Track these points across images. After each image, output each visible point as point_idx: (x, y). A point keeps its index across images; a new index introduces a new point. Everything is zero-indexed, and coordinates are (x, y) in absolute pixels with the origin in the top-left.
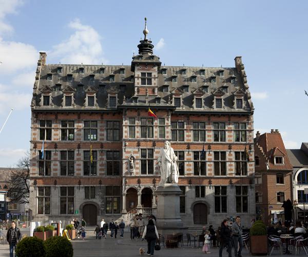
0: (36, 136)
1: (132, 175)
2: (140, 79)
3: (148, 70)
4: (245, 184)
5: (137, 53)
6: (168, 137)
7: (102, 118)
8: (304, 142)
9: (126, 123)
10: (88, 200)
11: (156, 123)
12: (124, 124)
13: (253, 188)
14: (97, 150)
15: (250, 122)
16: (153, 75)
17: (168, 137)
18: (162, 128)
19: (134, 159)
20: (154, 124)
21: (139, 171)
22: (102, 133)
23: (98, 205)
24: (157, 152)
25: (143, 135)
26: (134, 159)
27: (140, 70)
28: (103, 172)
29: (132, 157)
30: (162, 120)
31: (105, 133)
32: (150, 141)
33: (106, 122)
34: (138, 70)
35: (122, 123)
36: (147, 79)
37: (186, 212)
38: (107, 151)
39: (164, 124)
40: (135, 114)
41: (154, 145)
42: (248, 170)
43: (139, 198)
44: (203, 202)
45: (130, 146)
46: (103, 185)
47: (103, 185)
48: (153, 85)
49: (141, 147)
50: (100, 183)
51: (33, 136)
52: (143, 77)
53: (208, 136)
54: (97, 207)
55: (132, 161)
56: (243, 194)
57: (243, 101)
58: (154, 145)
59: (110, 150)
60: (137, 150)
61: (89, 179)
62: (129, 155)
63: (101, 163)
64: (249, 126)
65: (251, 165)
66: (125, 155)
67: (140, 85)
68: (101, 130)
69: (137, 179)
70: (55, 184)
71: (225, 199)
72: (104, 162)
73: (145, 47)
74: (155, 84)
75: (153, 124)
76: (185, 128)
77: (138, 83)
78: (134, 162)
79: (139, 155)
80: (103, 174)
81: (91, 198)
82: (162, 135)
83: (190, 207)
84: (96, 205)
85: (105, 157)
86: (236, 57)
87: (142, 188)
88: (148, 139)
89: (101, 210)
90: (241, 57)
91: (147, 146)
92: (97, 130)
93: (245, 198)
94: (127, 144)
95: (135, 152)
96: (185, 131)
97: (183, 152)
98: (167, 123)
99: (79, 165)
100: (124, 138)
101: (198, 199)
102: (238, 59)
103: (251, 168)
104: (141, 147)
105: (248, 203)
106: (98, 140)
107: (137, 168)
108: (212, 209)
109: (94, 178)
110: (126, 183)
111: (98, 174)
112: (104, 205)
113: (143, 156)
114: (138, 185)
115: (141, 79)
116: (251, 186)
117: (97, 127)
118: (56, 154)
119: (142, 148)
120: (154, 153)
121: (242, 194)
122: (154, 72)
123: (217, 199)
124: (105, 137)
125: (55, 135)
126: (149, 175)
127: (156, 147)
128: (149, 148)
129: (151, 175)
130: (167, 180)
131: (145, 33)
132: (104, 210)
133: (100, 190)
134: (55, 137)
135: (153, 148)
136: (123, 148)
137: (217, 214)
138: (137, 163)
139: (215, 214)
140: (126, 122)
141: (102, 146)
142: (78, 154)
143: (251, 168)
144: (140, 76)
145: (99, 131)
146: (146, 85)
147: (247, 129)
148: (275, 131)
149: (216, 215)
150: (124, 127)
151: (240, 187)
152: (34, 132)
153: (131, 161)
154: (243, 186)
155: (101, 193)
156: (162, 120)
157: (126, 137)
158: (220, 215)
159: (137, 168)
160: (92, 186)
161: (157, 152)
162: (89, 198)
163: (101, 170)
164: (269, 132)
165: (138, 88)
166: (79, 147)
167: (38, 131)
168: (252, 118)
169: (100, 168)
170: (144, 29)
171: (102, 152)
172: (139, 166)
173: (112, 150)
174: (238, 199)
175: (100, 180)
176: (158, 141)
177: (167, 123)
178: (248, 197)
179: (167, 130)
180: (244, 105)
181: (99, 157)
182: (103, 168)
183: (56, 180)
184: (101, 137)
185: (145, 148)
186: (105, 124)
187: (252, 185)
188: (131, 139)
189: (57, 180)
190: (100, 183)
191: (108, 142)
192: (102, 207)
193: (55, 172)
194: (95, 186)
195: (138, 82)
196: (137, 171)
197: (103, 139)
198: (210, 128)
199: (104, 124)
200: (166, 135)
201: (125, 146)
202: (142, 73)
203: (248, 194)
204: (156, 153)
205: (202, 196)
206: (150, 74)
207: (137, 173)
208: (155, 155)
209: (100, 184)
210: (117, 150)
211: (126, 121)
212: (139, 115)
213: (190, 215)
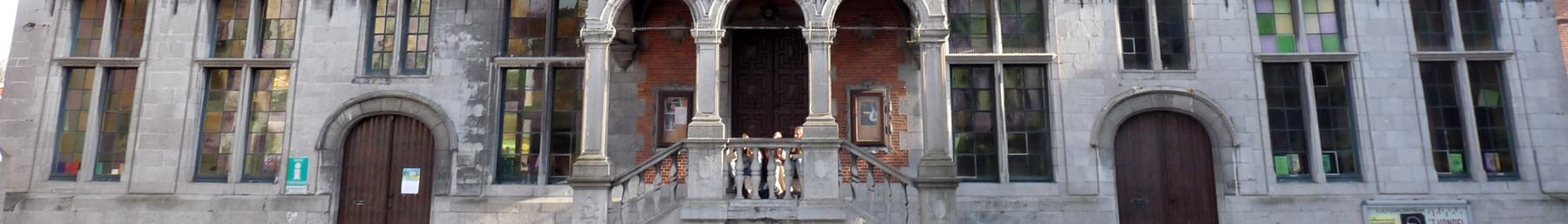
10: (379, 87)
23: (444, 119)
37: (1059, 175)
43: (709, 63)
44: (1177, 103)
54: (439, 133)
56: (1469, 42)
81: (405, 70)
83: (1086, 137)
84: (431, 121)
89: (461, 160)
93: (1489, 74)
101: (1138, 82)
105: (1517, 106)
108: (1249, 158)
112: (481, 121)
121: (1458, 45)
123: (1280, 78)
132: (480, 158)
137: (1298, 189)
139: (1277, 190)
149: (1289, 200)
155: (467, 41)
158: (1315, 199)
162: (385, 74)
174: (1437, 78)
192: (472, 139)
205: (1168, 61)
213: (1087, 199)
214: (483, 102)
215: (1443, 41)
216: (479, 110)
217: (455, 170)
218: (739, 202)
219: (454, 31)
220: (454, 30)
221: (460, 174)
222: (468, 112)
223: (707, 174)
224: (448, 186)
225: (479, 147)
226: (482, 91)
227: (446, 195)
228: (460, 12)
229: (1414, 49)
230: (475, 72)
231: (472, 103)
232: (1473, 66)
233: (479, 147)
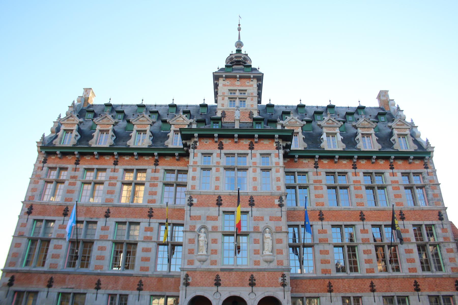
4: (447, 290)
9: (194, 162)
12: (191, 163)
26: (207, 232)
27: (228, 86)
29: (204, 227)
34: (224, 85)
45: (201, 204)
77: (223, 105)
87: (225, 296)
94: (195, 201)
95: (209, 218)
99: (102, 249)
104: (222, 209)
114: (215, 288)
131: (239, 44)
142: (105, 228)
144: (227, 93)
166: (107, 215)
170: (237, 40)
193: (54, 261)
199: (160, 175)
211: (196, 159)
212: (221, 147)
228: (137, 301)
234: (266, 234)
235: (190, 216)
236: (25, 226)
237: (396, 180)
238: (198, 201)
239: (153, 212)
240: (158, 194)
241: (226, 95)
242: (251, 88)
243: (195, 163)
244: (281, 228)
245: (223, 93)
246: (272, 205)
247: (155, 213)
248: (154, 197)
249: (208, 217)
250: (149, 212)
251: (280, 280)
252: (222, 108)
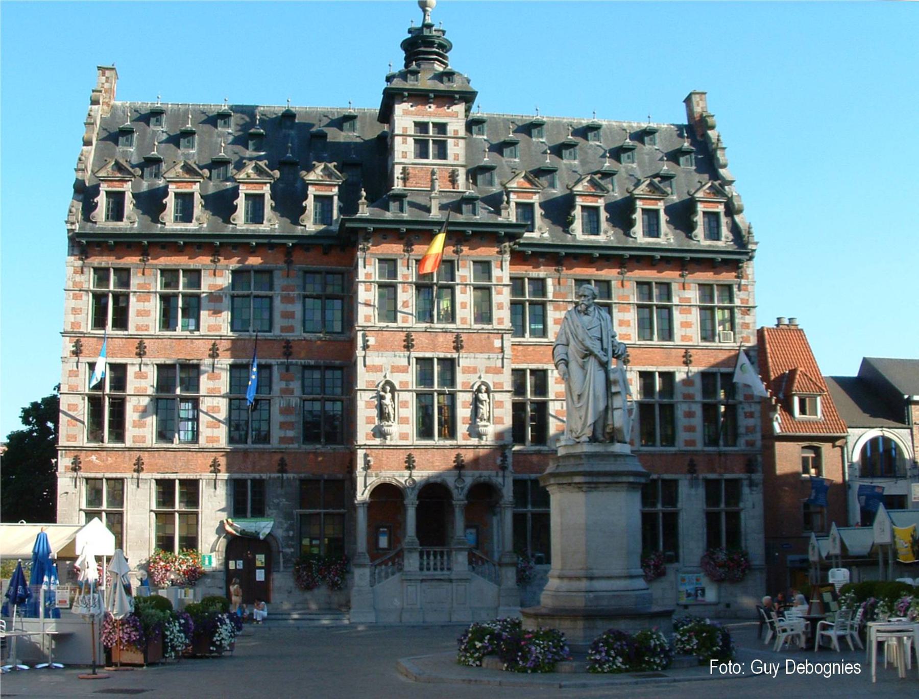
0: (81, 318)
1: (388, 442)
2: (411, 141)
3: (435, 115)
4: (733, 472)
5: (399, 65)
6: (501, 321)
7: (289, 262)
8: (866, 356)
11: (463, 277)
12: (361, 277)
13: (757, 486)
14: (273, 362)
15: (743, 282)
16: (450, 129)
17: (501, 321)
18: (484, 291)
19: (393, 390)
20: (458, 281)
21: (411, 429)
22: (290, 308)
24: (467, 370)
25: (425, 314)
28: (290, 434)
30: (484, 267)
31: (297, 308)
32: (445, 331)
33: (301, 273)
34: (406, 113)
35: (357, 276)
36: (431, 141)
38: (305, 367)
39: (490, 279)
40: (394, 249)
41: (458, 347)
42: (742, 430)
45: (381, 347)
46: (291, 476)
47: (291, 476)
48: (450, 160)
49: (415, 354)
50: (282, 468)
51: (72, 318)
52: (421, 137)
53: (622, 323)
55: (388, 396)
57: (724, 220)
58: (458, 347)
59: (312, 362)
60: (404, 362)
61: (246, 452)
62: (379, 378)
63: (283, 403)
64: (742, 295)
65: (751, 415)
66: (363, 378)
67: (411, 158)
68: (287, 299)
69: (403, 456)
70: (138, 471)
71: (671, 521)
72: (294, 401)
73: (421, 46)
74: (456, 157)
75: (453, 279)
76: (550, 296)
77: (404, 155)
78: (393, 398)
79: (410, 377)
80: (291, 440)
82: (484, 315)
85: (296, 385)
86: (691, 94)
88: (437, 325)
89: (285, 555)
90: (705, 93)
91: (434, 350)
92: (271, 298)
93: (734, 518)
94: (372, 341)
95: (396, 369)
96: (550, 308)
97: (544, 372)
98: (500, 279)
100: (361, 321)
102: (695, 99)
103: (751, 422)
104: (415, 354)
106: (277, 331)
107: (404, 421)
109: (262, 452)
110: (367, 466)
111: (275, 442)
112: (292, 538)
113: (425, 377)
115: (416, 141)
116: (750, 479)
117: (271, 288)
118: (140, 375)
119: (421, 355)
120: (459, 370)
121: (723, 506)
122: (454, 118)
124: (297, 323)
125: (139, 313)
126: (441, 443)
127: (463, 354)
128: (442, 355)
129: (448, 442)
130: (588, 432)
133: (279, 491)
134: (141, 321)
135: (455, 355)
136: (360, 353)
138: (405, 404)
140: (368, 270)
141: (288, 348)
143: (751, 422)
144: (411, 130)
145: (277, 302)
146: (431, 160)
147: (737, 302)
148: (787, 322)
150: (361, 288)
151: (717, 481)
152: (73, 303)
153: (382, 398)
154: (726, 480)
156: (484, 267)
157: (367, 318)
159: (404, 421)
160: (257, 476)
161: (467, 370)
163: (283, 425)
164: (772, 324)
165: (404, 169)
167: (87, 303)
168: (749, 271)
169: (282, 419)
171: (287, 370)
172: (410, 412)
173: (321, 362)
174: (712, 520)
175: (282, 460)
176: (470, 331)
177: (500, 279)
178: (743, 515)
179: (496, 298)
180: (725, 231)
181: (278, 385)
182: (292, 418)
183: (139, 459)
184: (286, 323)
185: (428, 355)
186: (299, 282)
187: (754, 476)
188: (385, 324)
189: (145, 456)
190: (282, 468)
191: (308, 336)
192: (289, 546)
194: (264, 476)
195: (403, 150)
196: (403, 428)
197: (291, 329)
198: (628, 297)
199: (296, 281)
200: (496, 314)
201: (366, 347)
202: (417, 124)
203: (741, 505)
204: (463, 373)
206: (441, 128)
207: (404, 436)
208: (460, 378)
209: (279, 472)
210: (337, 362)
211: (369, 269)
214: (293, 530)
215: (717, 503)
216: (291, 533)
217: (281, 560)
218: (425, 572)
219: (277, 497)
220: (278, 497)
221: (284, 562)
222: (284, 534)
223: (412, 562)
224: (279, 567)
225: (292, 550)
226: (291, 525)
227: (278, 571)
229: (705, 507)
230: (288, 516)
231: (287, 530)
232: (727, 513)
233: (292, 550)
234: (480, 395)
235: (365, 366)
236: (77, 376)
237: (687, 296)
238: (376, 342)
239: (291, 347)
240: (296, 316)
241: (408, 133)
242: (454, 120)
243: (368, 275)
244: (501, 384)
245: (405, 129)
246: (490, 349)
247: (295, 349)
248: (290, 322)
249: (393, 367)
250: (284, 347)
251: (499, 462)
252: (403, 160)
